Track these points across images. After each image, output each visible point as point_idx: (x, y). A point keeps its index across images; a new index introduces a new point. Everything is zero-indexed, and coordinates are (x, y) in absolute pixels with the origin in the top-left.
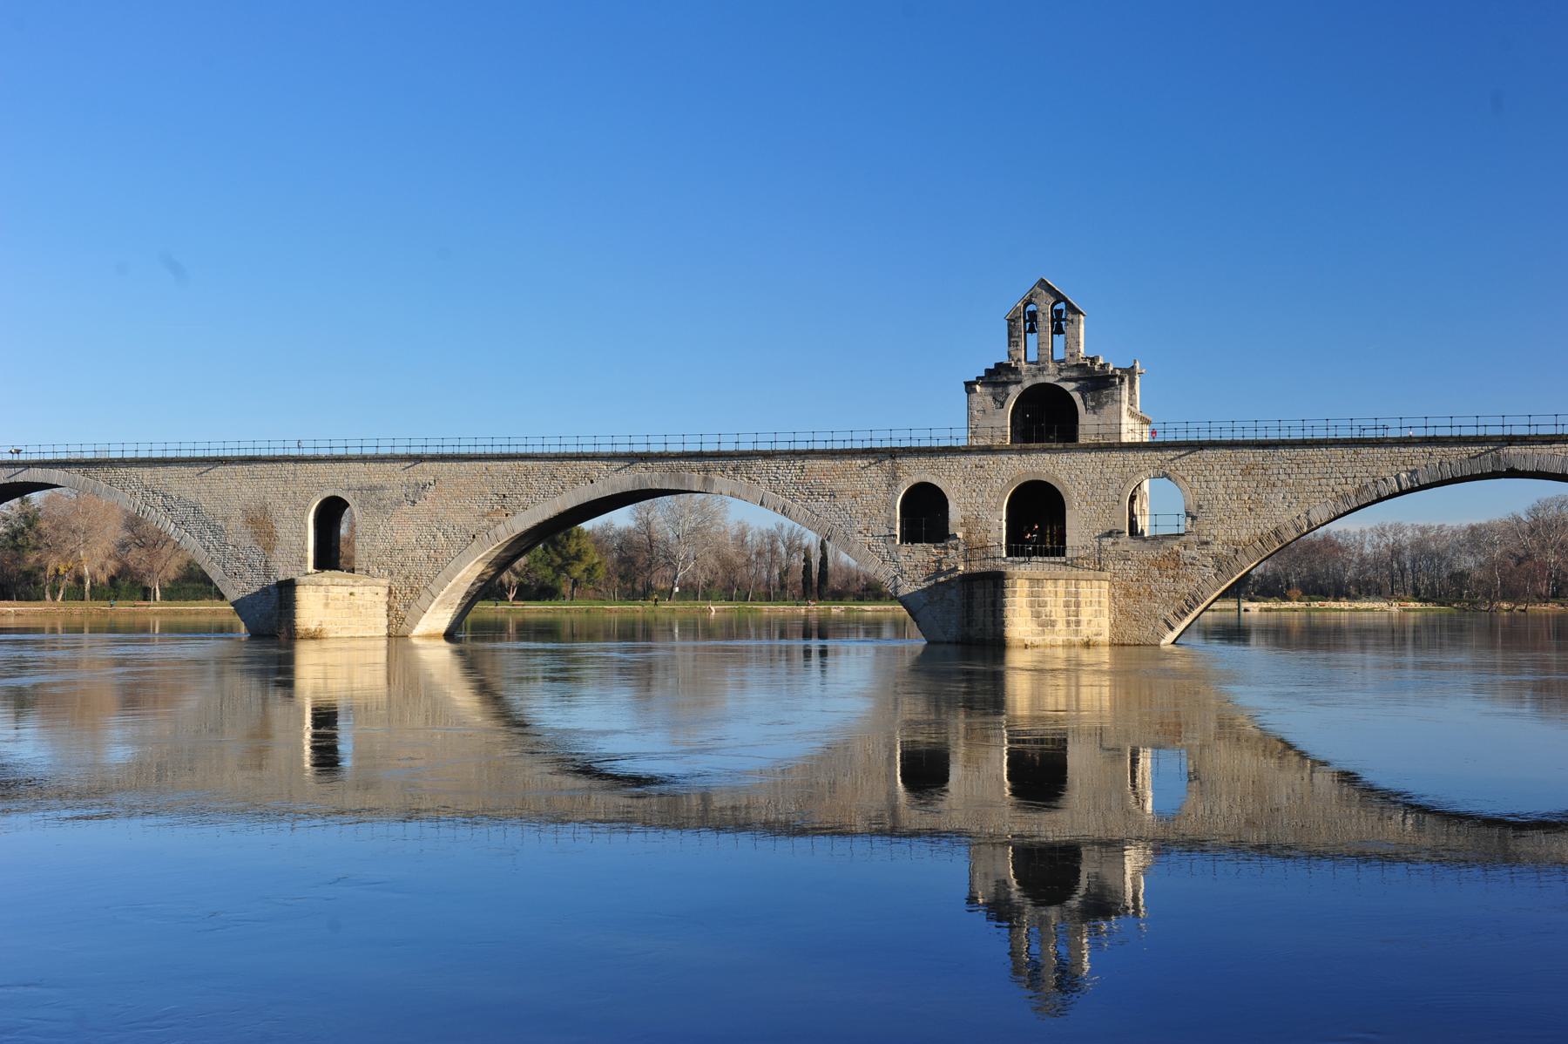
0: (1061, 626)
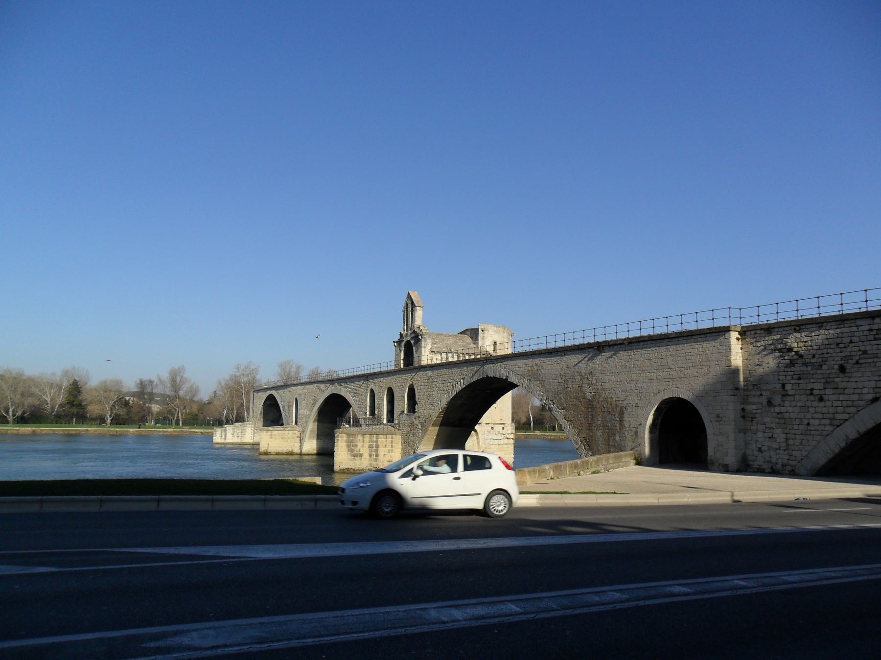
0: (366, 455)
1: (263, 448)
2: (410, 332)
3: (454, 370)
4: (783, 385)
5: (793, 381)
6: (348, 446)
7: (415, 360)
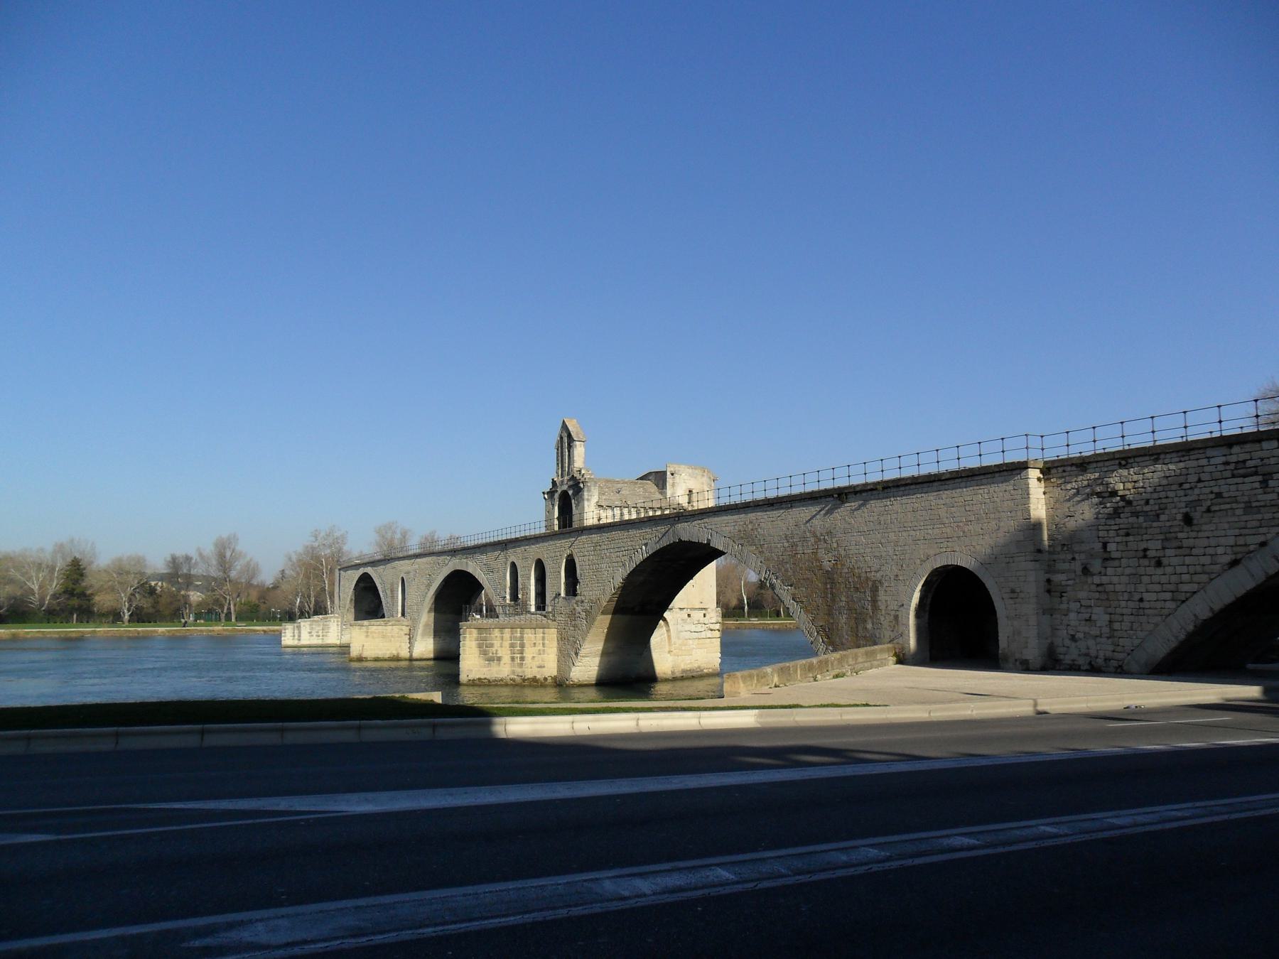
0: (506, 659)
1: (354, 652)
2: (566, 478)
3: (632, 532)
4: (1105, 545)
5: (1118, 539)
6: (480, 646)
7: (575, 518)
